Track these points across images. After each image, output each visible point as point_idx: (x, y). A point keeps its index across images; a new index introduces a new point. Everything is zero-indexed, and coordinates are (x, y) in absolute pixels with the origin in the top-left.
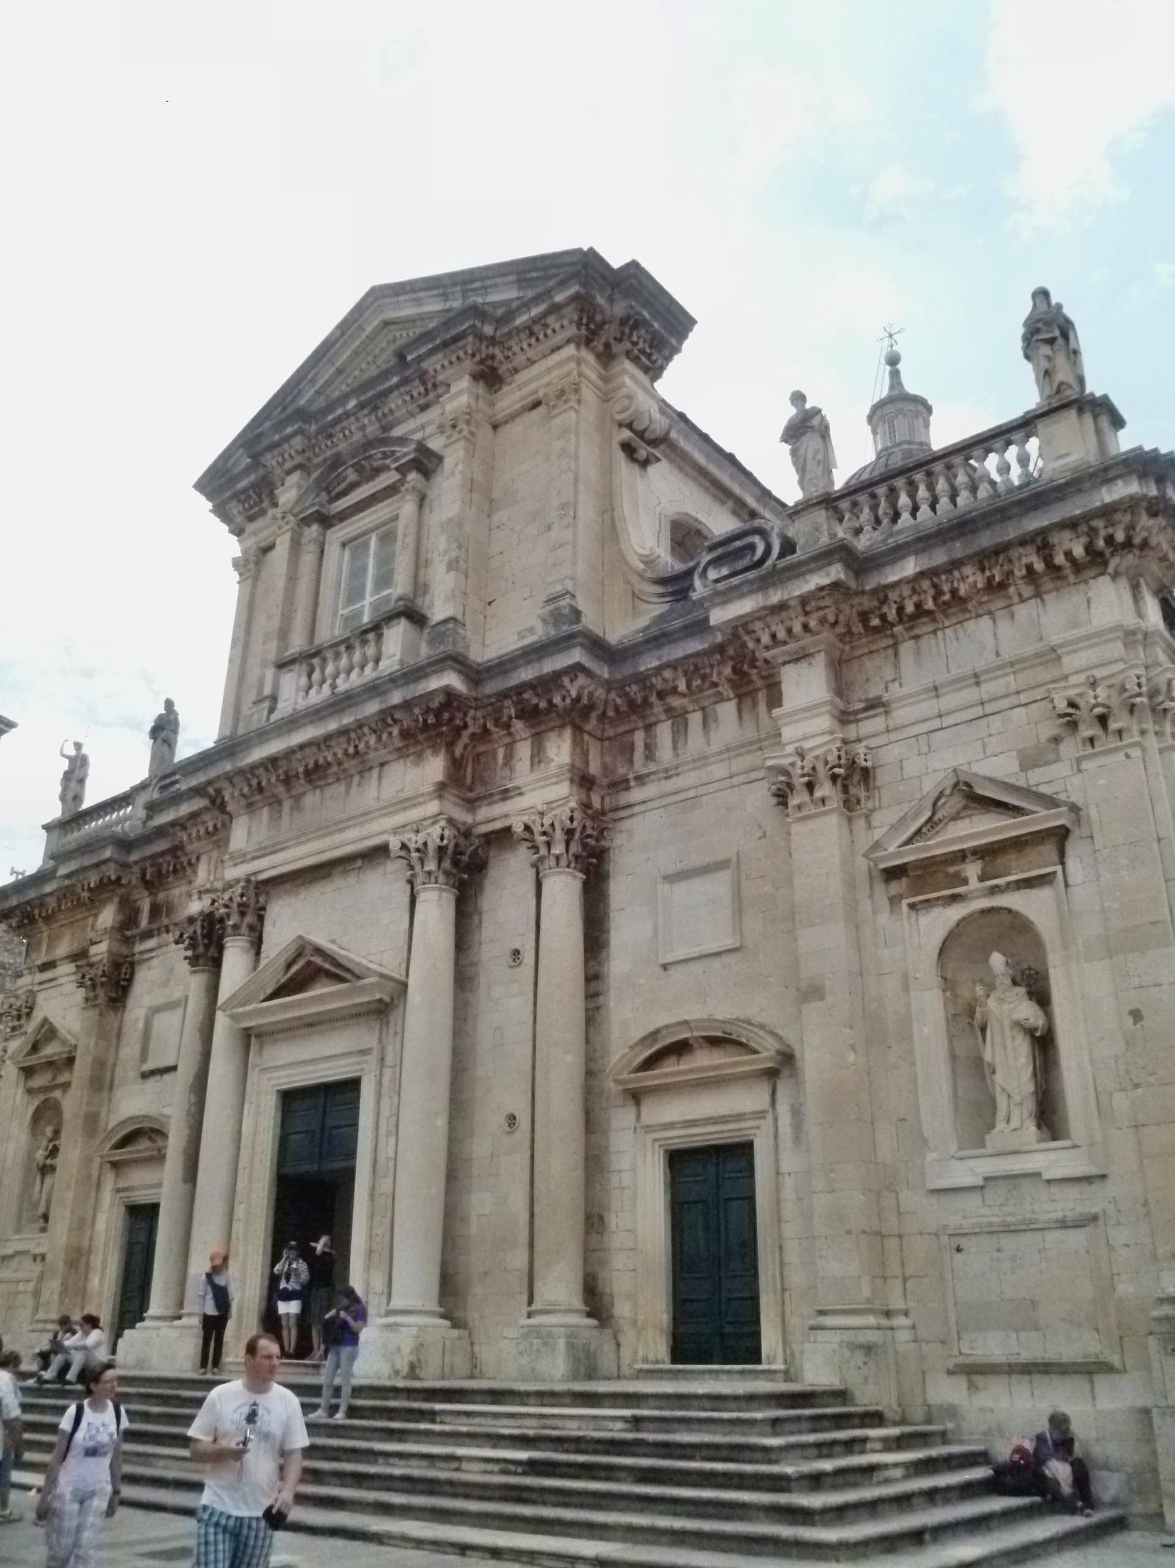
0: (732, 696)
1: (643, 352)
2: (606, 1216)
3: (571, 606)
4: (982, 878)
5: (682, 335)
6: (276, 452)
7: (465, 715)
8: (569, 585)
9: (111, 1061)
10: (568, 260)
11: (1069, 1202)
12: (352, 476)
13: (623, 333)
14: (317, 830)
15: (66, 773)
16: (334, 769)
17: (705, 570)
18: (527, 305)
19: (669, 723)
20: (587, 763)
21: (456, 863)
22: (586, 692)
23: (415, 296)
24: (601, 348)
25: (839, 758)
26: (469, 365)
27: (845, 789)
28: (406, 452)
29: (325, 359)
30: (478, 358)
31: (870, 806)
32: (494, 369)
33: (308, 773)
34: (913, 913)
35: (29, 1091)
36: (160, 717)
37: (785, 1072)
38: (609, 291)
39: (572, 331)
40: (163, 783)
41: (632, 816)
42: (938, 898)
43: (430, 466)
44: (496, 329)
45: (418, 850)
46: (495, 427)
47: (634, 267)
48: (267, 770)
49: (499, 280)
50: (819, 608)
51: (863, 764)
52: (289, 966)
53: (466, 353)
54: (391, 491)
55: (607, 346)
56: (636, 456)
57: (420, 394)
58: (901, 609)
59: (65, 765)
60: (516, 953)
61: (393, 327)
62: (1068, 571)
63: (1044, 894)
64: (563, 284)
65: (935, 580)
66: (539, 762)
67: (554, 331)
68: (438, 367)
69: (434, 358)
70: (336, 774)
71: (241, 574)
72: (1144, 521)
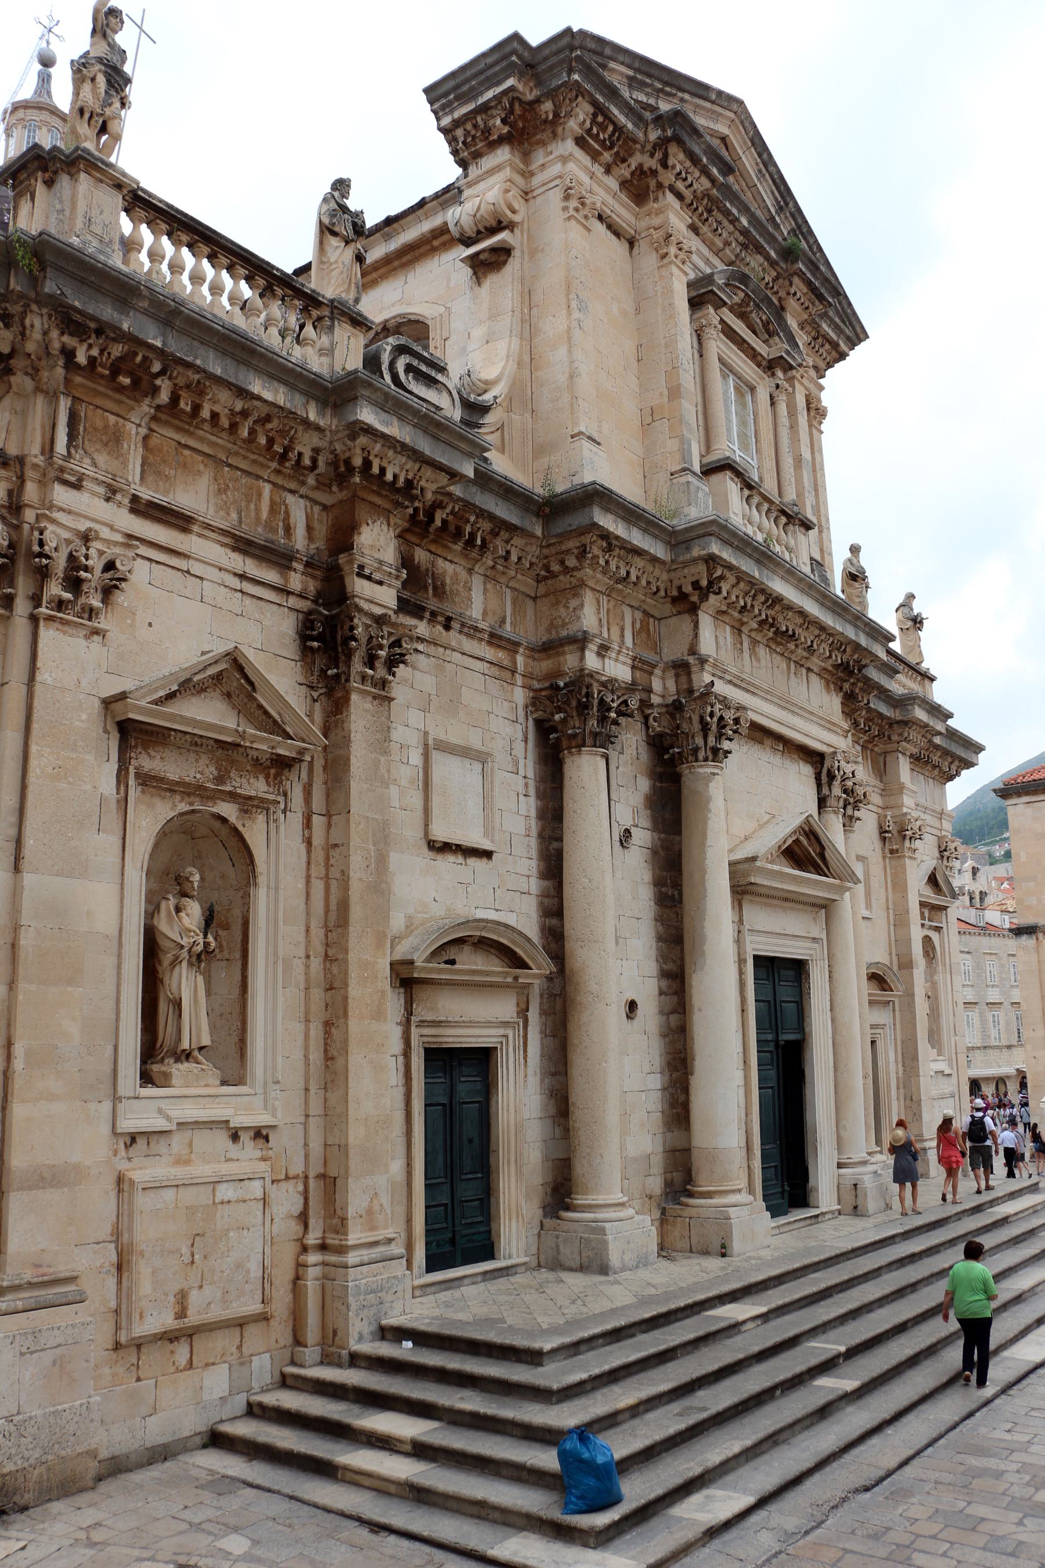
6: (688, 164)
14: (780, 698)
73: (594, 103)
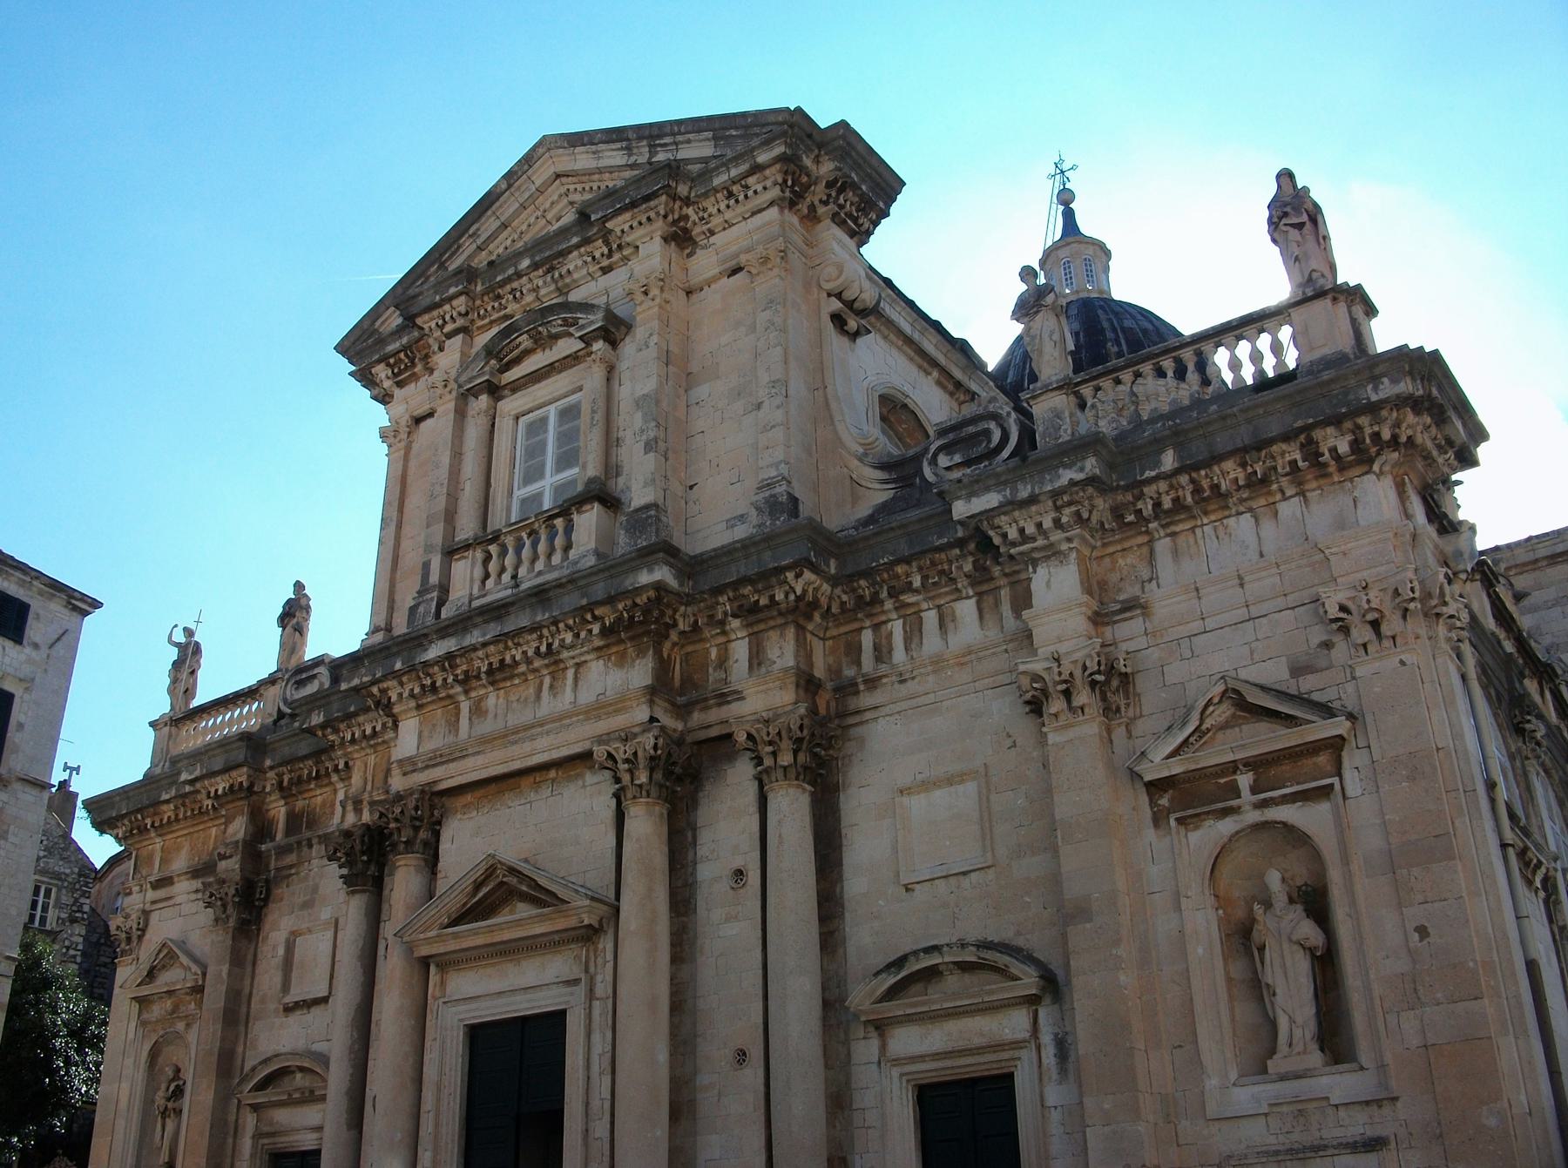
0: (971, 593)
1: (849, 215)
2: (849, 1157)
3: (789, 493)
4: (1255, 790)
5: (891, 199)
6: (435, 313)
7: (675, 611)
8: (784, 469)
9: (247, 991)
10: (771, 119)
11: (1357, 1125)
12: (525, 341)
13: (829, 196)
15: (174, 663)
16: (522, 668)
17: (935, 455)
18: (726, 165)
19: (901, 621)
20: (811, 665)
21: (668, 774)
22: (810, 590)
23: (594, 148)
24: (806, 211)
25: (1099, 663)
26: (659, 226)
27: (1104, 699)
28: (596, 321)
29: (489, 212)
30: (670, 218)
31: (1131, 713)
32: (686, 231)
33: (490, 672)
34: (1182, 830)
35: (143, 1023)
36: (289, 601)
37: (1047, 1000)
38: (816, 151)
39: (775, 192)
40: (298, 678)
41: (861, 723)
42: (1208, 812)
43: (618, 336)
44: (691, 188)
45: (627, 761)
46: (689, 293)
47: (843, 129)
48: (444, 669)
49: (691, 136)
50: (1070, 504)
51: (1123, 670)
52: (478, 886)
53: (658, 214)
54: (573, 360)
55: (812, 208)
56: (845, 328)
57: (603, 255)
58: (1157, 505)
59: (173, 654)
60: (739, 874)
61: (564, 180)
62: (1332, 468)
63: (1323, 808)
64: (767, 143)
65: (1194, 475)
66: (759, 664)
67: (755, 192)
68: (626, 227)
69: (620, 219)
70: (523, 674)
71: (390, 446)
72: (1411, 418)
73: (379, 361)
